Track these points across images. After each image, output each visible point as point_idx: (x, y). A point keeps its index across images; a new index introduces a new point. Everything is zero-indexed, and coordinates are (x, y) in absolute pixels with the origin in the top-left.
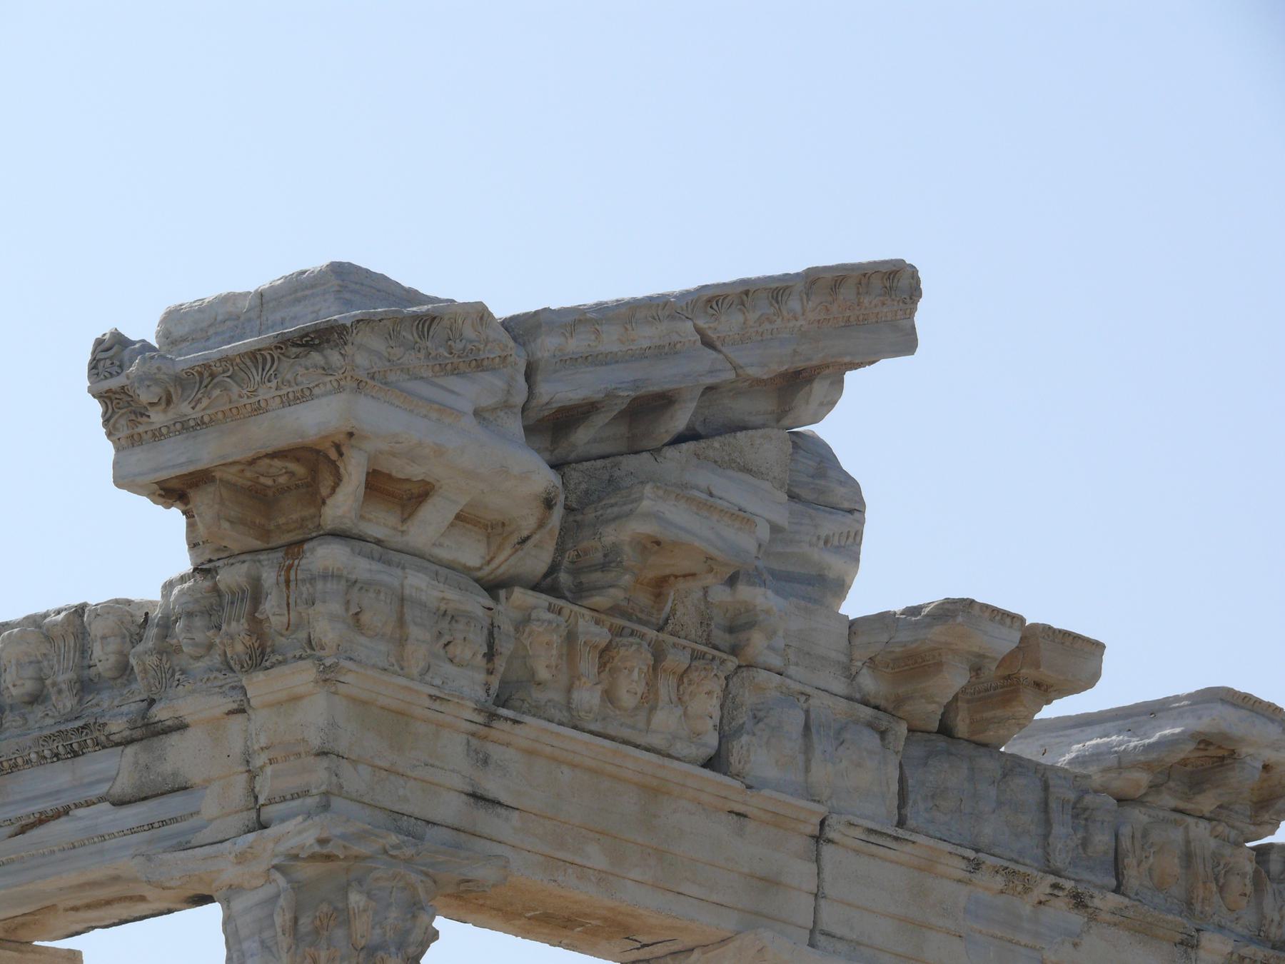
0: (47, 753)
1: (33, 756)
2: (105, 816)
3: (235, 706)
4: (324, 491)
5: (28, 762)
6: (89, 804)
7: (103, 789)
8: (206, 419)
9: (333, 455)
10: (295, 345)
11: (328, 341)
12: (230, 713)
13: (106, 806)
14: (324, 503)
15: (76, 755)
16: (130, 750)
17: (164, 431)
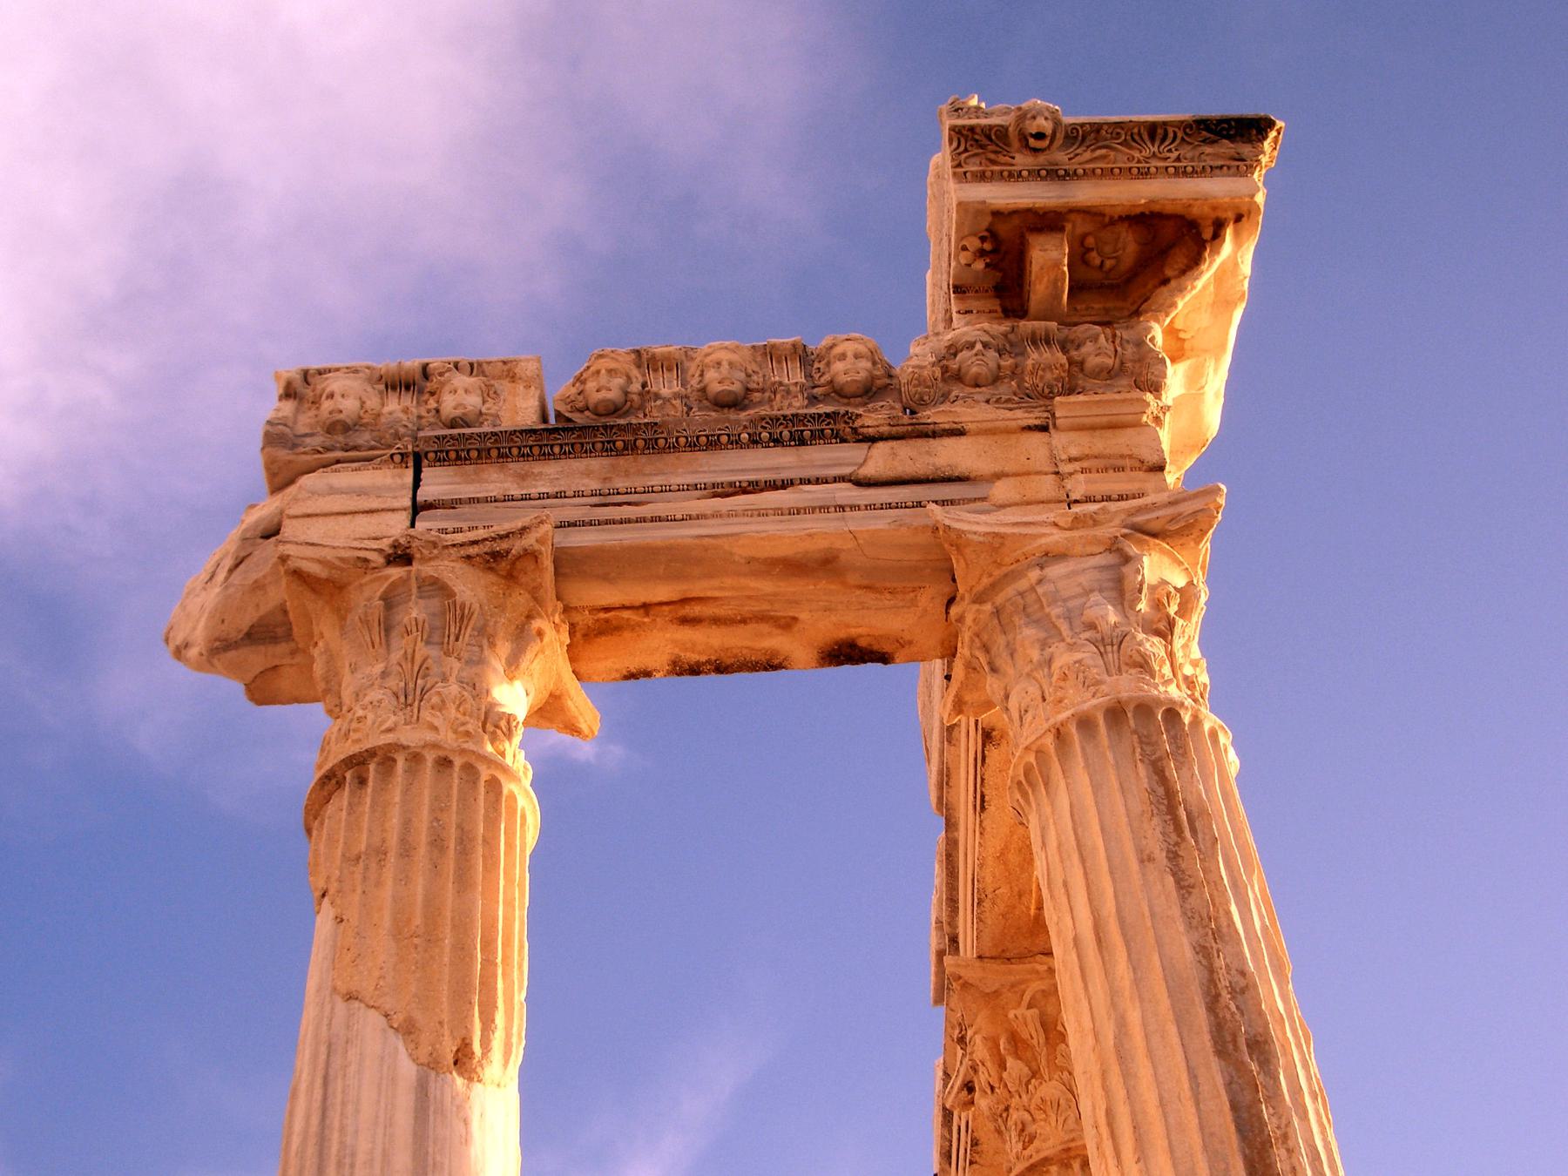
0: (765, 435)
1: (745, 436)
2: (846, 493)
3: (1037, 422)
4: (1169, 272)
5: (735, 443)
6: (818, 481)
7: (846, 471)
8: (1080, 171)
9: (1207, 234)
10: (1208, 129)
11: (1242, 136)
12: (1029, 428)
13: (849, 485)
14: (1165, 282)
15: (802, 442)
16: (881, 447)
17: (1025, 173)
